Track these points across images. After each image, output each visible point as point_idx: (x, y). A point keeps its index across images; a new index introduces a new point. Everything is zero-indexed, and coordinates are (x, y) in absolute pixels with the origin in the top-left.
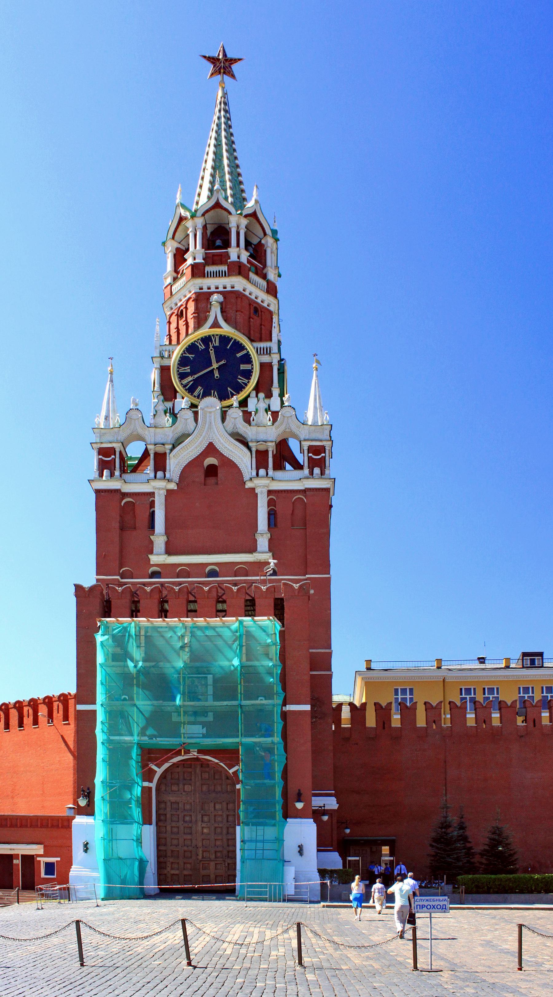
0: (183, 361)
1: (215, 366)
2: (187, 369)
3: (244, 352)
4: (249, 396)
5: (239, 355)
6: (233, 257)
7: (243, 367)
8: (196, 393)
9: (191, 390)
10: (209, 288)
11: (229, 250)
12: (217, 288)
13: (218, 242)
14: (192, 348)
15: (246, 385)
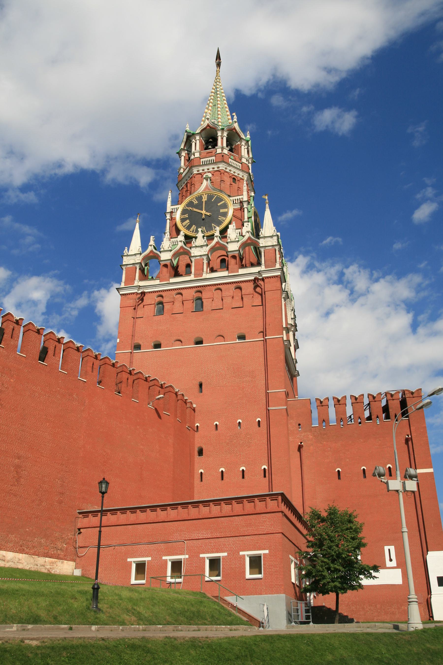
0: (184, 212)
1: (204, 212)
2: (186, 216)
3: (223, 202)
4: (227, 228)
5: (219, 204)
6: (219, 151)
7: (222, 211)
8: (191, 230)
9: (188, 228)
10: (203, 170)
11: (216, 147)
12: (208, 169)
13: (210, 147)
14: (190, 204)
15: (224, 221)
